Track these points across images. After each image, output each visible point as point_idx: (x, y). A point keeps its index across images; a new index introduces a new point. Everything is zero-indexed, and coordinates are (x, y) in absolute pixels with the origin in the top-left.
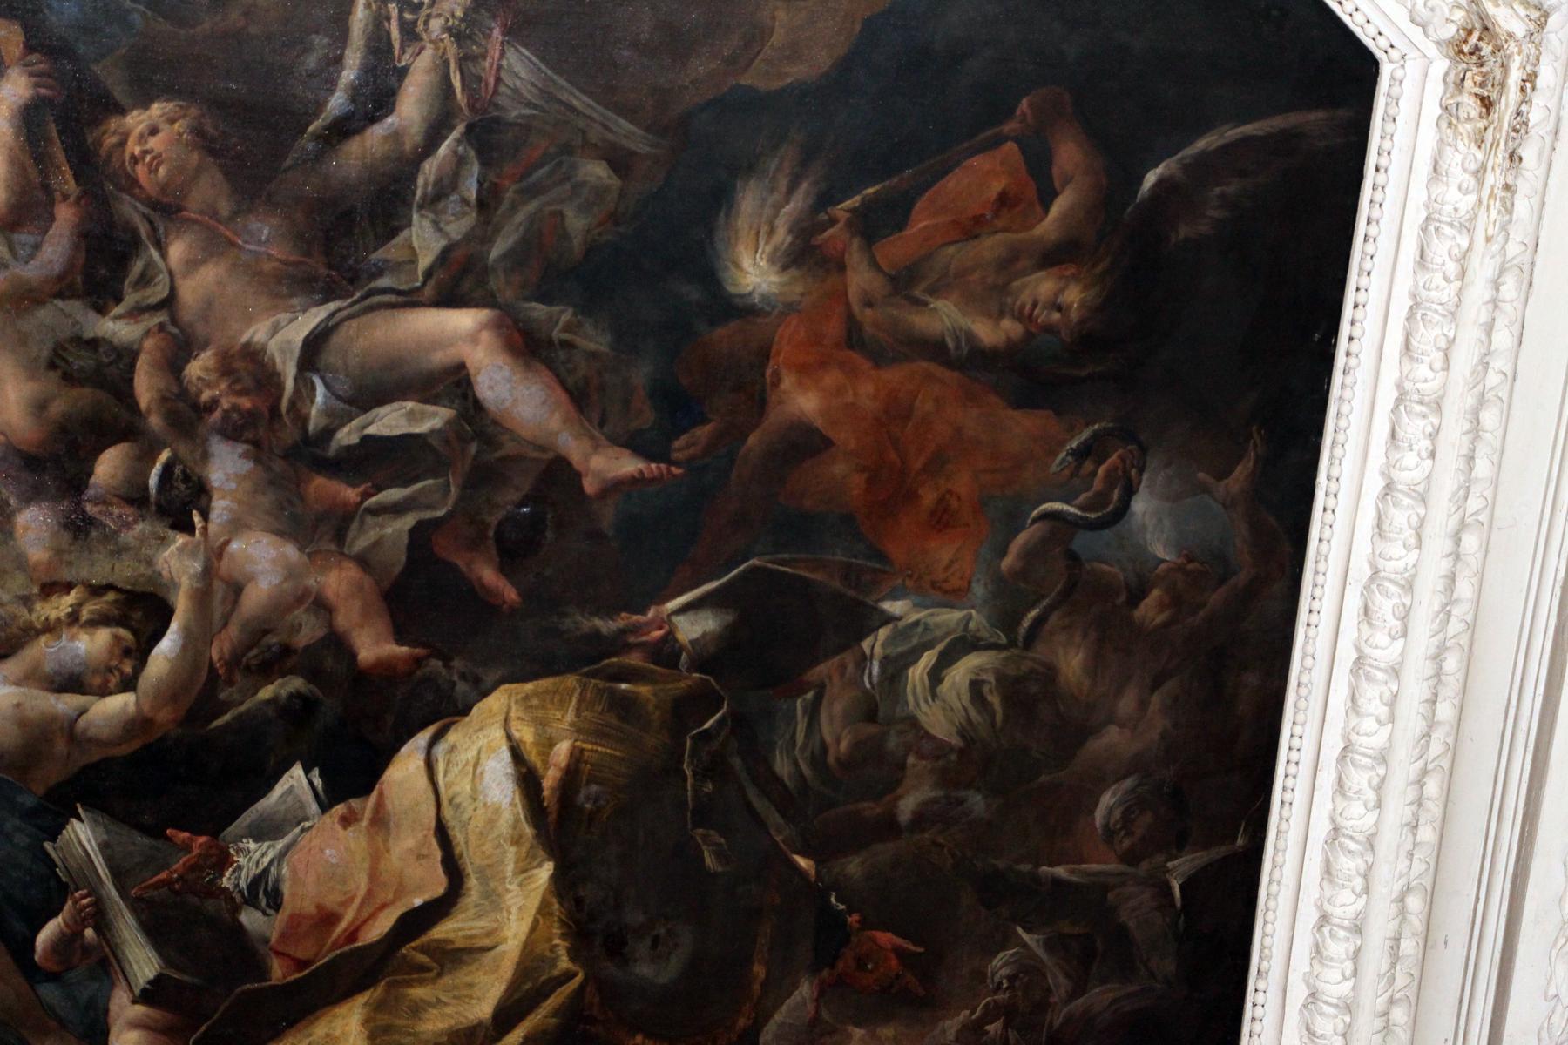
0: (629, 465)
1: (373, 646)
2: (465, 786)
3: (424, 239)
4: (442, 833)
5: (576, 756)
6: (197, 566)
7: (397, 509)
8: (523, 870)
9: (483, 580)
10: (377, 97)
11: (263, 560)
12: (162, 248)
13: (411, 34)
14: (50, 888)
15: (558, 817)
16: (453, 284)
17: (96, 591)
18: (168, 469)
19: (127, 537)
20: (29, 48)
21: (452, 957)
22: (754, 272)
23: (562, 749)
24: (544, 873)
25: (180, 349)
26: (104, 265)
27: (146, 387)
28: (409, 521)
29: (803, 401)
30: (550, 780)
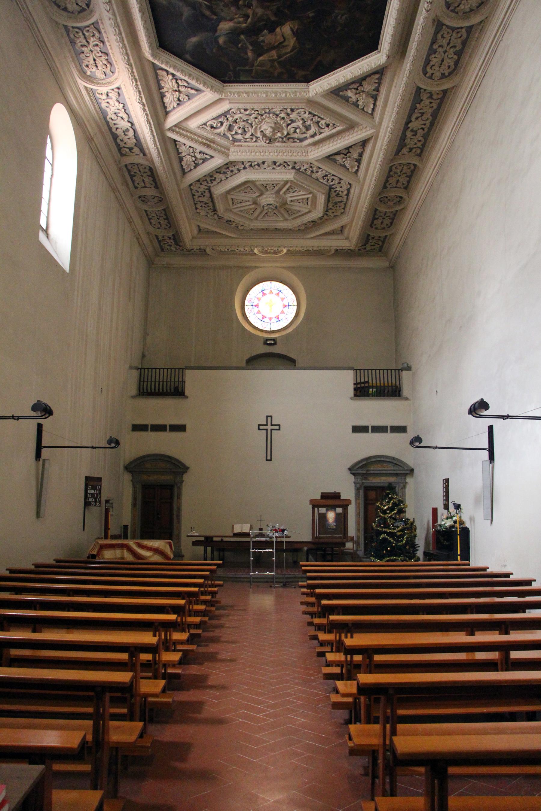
1: (273, 18)
4: (283, 36)
5: (298, 29)
7: (275, 5)
8: (292, 38)
11: (260, 11)
15: (295, 33)
17: (241, 14)
21: (285, 46)
23: (296, 27)
24: (295, 39)
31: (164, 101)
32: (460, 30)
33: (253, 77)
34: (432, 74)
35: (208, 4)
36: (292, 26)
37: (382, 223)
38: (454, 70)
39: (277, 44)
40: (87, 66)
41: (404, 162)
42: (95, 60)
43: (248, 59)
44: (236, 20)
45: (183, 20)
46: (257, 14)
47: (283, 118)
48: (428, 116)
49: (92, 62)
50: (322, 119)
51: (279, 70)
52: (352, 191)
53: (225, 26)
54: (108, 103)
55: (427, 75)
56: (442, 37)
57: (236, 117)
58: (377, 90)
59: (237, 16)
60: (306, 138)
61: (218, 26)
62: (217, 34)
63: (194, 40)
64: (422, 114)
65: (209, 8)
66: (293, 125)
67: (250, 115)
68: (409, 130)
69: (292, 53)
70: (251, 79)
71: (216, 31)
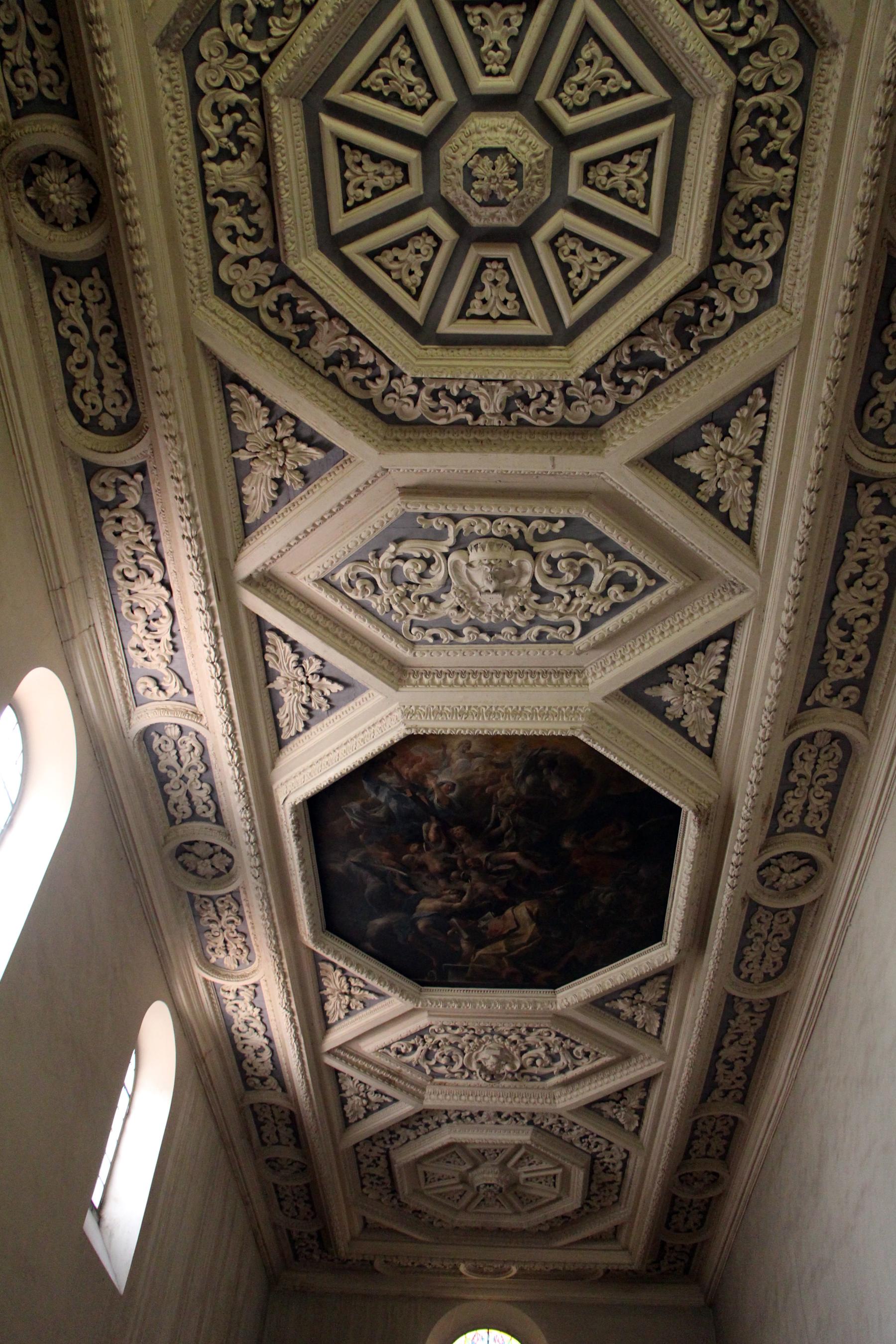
0: (545, 872)
1: (501, 896)
3: (506, 843)
4: (516, 920)
10: (497, 822)
11: (481, 886)
15: (534, 917)
16: (513, 848)
21: (517, 935)
25: (464, 859)
26: (452, 846)
27: (459, 863)
34: (750, 975)
37: (686, 1220)
38: (782, 970)
39: (505, 932)
40: (213, 950)
41: (717, 1113)
42: (225, 942)
43: (461, 950)
47: (515, 1042)
49: (221, 944)
50: (578, 1044)
52: (631, 1163)
53: (427, 905)
54: (236, 1005)
55: (742, 976)
56: (759, 921)
57: (438, 1037)
58: (665, 999)
60: (552, 1075)
61: (418, 903)
62: (415, 915)
63: (379, 922)
64: (740, 1035)
66: (531, 1053)
67: (460, 1035)
68: (721, 1061)
70: (463, 981)
71: (414, 911)
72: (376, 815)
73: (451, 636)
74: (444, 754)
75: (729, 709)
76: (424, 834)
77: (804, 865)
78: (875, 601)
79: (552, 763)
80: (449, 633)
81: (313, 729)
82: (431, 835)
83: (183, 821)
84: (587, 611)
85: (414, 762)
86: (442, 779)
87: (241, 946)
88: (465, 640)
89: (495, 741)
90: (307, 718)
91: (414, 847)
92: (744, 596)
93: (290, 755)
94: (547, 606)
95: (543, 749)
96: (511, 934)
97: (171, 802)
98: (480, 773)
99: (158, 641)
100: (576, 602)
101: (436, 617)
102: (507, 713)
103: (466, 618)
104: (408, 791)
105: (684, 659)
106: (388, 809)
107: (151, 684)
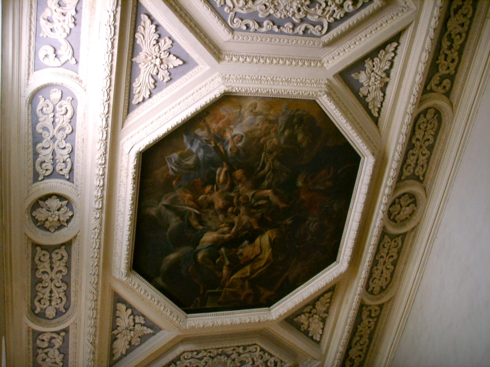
1: (256, 227)
2: (263, 241)
3: (266, 183)
4: (261, 247)
5: (275, 237)
6: (238, 220)
7: (259, 212)
9: (267, 219)
12: (238, 185)
13: (267, 161)
14: (218, 256)
15: (273, 244)
17: (227, 223)
18: (236, 210)
19: (231, 217)
20: (227, 165)
22: (300, 184)
23: (274, 237)
24: (270, 250)
25: (239, 196)
26: (232, 187)
27: (235, 201)
28: (261, 213)
29: (303, 197)
30: (272, 240)
31: (114, 347)
32: (396, 239)
33: (219, 303)
34: (373, 288)
35: (197, 212)
36: (270, 235)
39: (253, 257)
40: (39, 301)
42: (51, 292)
43: (221, 278)
44: (221, 230)
45: (167, 234)
46: (242, 222)
48: (365, 339)
51: (248, 291)
53: (209, 237)
55: (369, 290)
58: (327, 312)
59: (223, 225)
61: (202, 237)
62: (198, 248)
63: (172, 256)
65: (198, 217)
67: (201, 359)
69: (265, 268)
71: (197, 244)
72: (188, 163)
73: (257, 26)
74: (240, 112)
75: (391, 90)
76: (217, 177)
77: (411, 203)
78: (465, 24)
79: (301, 121)
80: (256, 23)
81: (154, 97)
82: (221, 178)
83: (45, 177)
84: (331, 16)
85: (220, 119)
86: (236, 131)
87: (62, 295)
88: (264, 30)
89: (273, 102)
90: (153, 86)
91: (208, 189)
92: (410, 12)
93: (135, 116)
94: (313, 9)
95: (297, 110)
96: (257, 258)
97: (39, 160)
98: (259, 127)
99: (64, 15)
100: (327, 9)
101: (251, 11)
102: (282, 81)
103: (268, 14)
104: (212, 142)
105: (373, 54)
106: (197, 158)
107: (51, 51)
